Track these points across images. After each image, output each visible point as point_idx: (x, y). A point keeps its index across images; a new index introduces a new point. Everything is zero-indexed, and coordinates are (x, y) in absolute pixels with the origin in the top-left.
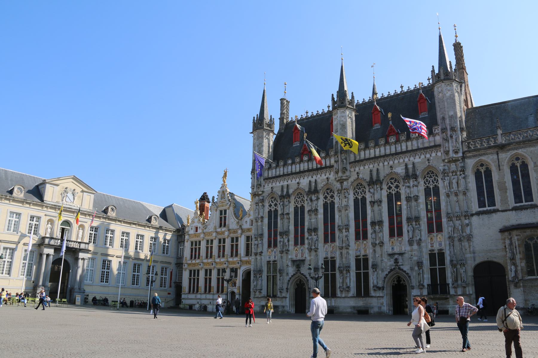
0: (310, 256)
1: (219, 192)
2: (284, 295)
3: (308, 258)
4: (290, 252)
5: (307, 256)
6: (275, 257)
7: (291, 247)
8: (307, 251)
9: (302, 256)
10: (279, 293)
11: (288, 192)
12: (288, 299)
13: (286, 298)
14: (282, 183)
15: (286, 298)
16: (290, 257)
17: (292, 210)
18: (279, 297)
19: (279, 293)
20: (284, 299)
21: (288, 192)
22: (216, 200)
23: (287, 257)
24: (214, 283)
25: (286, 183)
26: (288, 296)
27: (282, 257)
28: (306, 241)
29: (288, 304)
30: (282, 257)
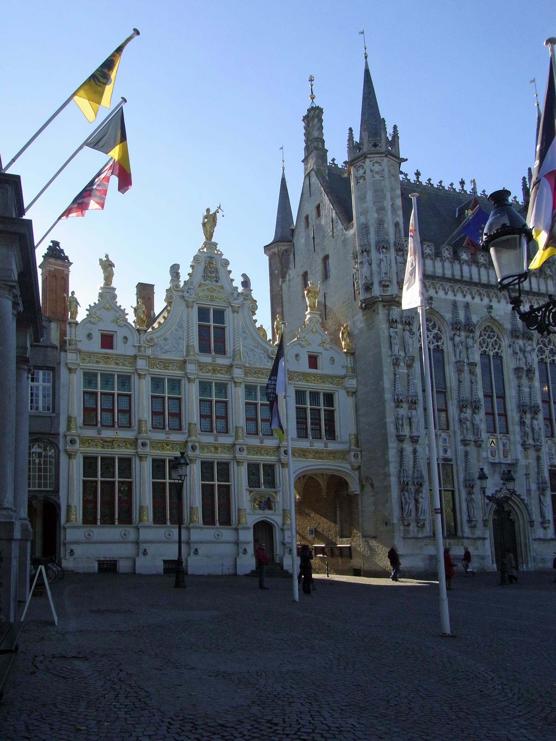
0: (526, 457)
1: (196, 258)
2: (478, 533)
3: (523, 462)
4: (483, 445)
5: (520, 457)
6: (445, 451)
7: (484, 435)
8: (519, 448)
9: (505, 456)
10: (466, 529)
11: (468, 318)
12: (488, 543)
13: (484, 539)
14: (450, 296)
15: (484, 539)
16: (484, 454)
17: (476, 357)
18: (468, 538)
19: (466, 529)
20: (480, 542)
21: (468, 318)
22: (184, 277)
23: (479, 454)
24: (194, 497)
25: (459, 297)
26: (487, 535)
27: (466, 454)
28: (515, 428)
29: (489, 553)
30: (466, 454)
